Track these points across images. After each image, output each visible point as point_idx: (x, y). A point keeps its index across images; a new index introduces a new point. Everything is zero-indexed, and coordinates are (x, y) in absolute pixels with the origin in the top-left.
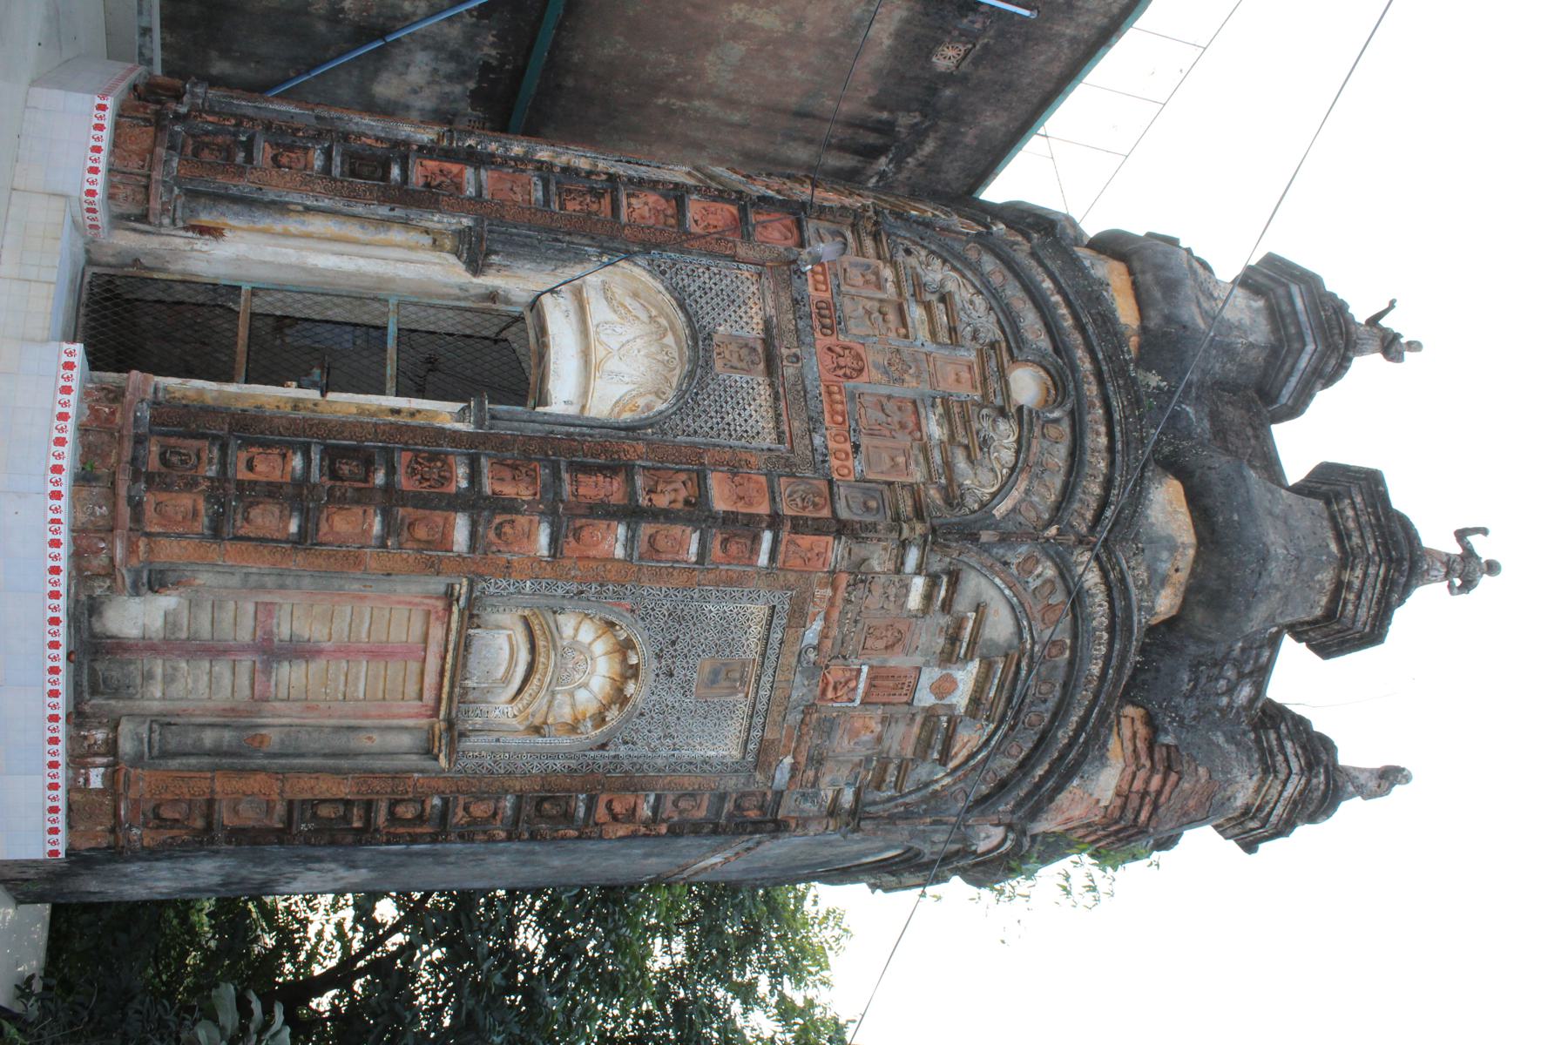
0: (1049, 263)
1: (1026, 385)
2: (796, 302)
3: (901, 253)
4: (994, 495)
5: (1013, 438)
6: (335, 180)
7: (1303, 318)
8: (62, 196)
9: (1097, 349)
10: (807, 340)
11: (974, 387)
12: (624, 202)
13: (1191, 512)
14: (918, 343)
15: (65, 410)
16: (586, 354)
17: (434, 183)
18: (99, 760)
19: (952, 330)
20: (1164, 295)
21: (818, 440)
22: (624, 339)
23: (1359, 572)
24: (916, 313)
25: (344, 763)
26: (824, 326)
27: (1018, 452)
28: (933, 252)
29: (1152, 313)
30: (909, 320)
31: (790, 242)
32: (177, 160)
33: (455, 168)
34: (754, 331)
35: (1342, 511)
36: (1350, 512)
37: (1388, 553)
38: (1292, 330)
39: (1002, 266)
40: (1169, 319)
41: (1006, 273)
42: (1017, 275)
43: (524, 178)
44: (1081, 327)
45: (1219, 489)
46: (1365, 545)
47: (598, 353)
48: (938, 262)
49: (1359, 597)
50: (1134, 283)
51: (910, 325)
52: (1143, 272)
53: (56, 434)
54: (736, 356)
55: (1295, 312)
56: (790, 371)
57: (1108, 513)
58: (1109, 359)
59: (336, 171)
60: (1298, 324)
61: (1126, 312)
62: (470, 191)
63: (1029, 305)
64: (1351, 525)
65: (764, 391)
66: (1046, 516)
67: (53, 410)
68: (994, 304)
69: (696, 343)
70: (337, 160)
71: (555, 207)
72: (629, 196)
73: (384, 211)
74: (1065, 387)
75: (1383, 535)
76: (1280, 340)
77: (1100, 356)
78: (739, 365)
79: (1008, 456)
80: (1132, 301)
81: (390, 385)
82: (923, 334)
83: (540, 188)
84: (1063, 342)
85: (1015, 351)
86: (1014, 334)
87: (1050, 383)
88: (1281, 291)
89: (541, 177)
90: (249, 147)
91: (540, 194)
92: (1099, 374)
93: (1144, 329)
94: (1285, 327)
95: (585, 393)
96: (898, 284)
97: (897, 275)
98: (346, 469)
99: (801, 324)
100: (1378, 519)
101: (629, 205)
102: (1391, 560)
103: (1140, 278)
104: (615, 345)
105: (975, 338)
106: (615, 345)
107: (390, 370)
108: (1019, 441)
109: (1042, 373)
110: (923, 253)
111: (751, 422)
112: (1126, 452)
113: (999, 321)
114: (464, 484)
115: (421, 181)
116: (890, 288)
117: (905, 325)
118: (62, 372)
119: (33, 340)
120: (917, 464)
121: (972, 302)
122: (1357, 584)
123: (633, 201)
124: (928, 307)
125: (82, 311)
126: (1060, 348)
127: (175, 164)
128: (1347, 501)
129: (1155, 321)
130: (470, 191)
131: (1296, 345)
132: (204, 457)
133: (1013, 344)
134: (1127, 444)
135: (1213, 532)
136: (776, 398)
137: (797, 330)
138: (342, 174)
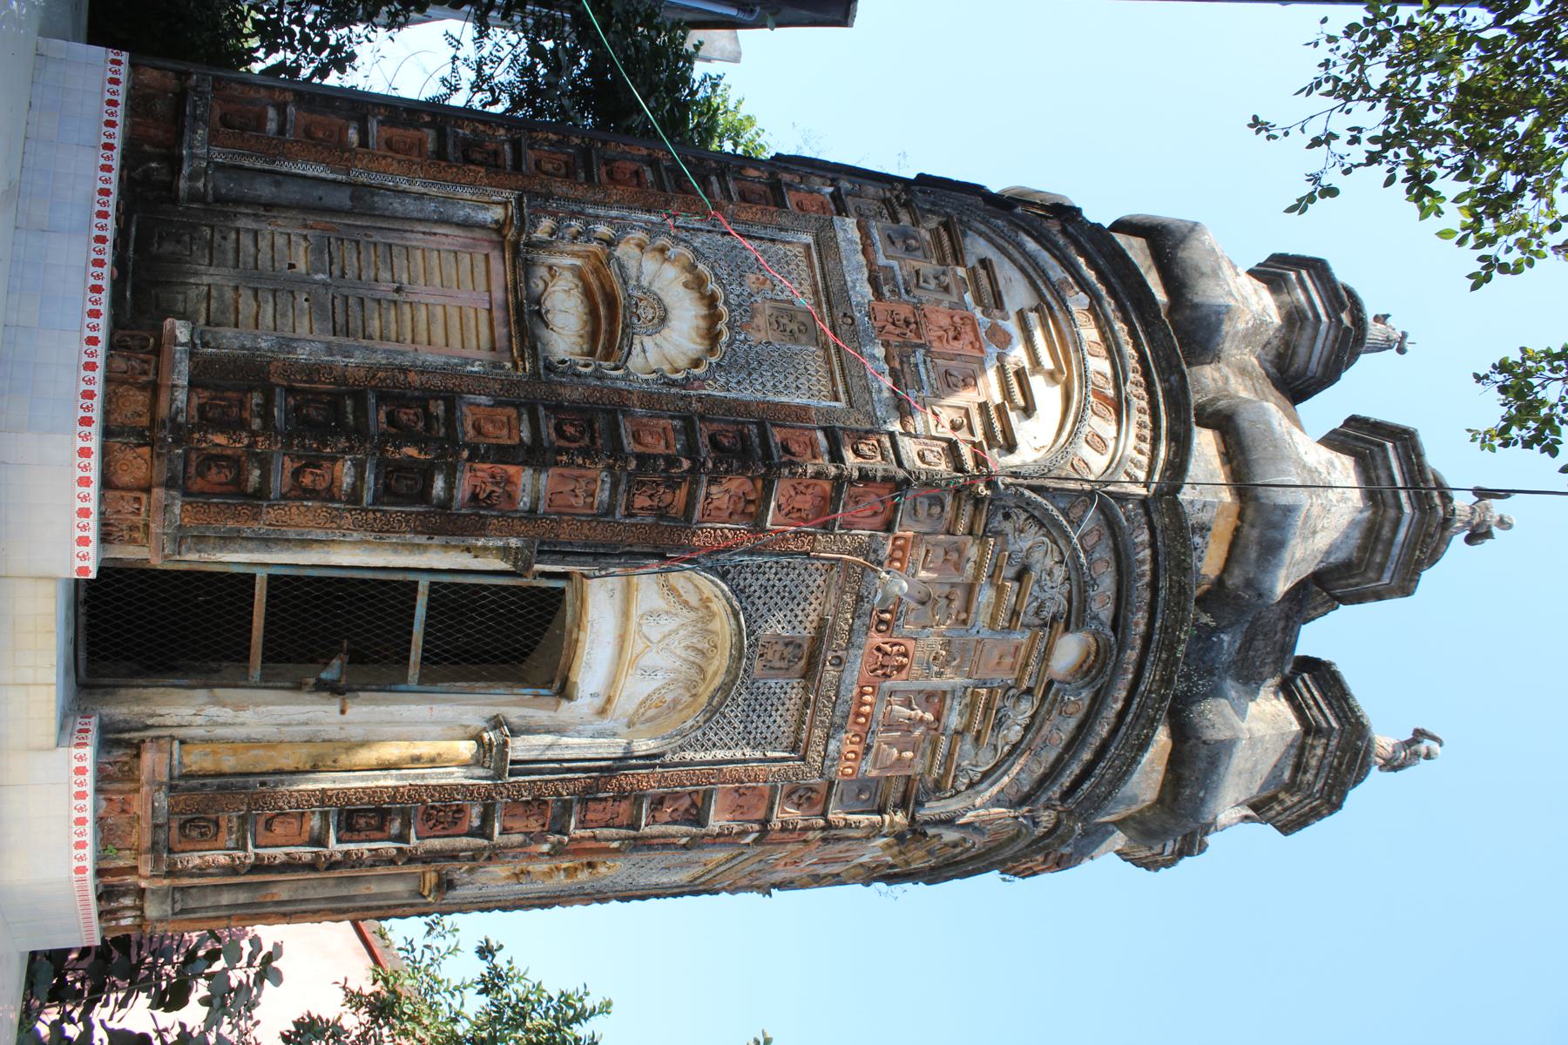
0: (1155, 517)
1: (1069, 650)
2: (860, 599)
3: (1000, 517)
4: (985, 775)
5: (1029, 713)
6: (366, 511)
7: (1396, 551)
8: (50, 578)
9: (1159, 616)
10: (857, 640)
11: (1012, 668)
12: (703, 492)
13: (1167, 771)
14: (974, 631)
15: (82, 815)
16: (622, 639)
17: (482, 496)
18: (129, 913)
19: (1015, 613)
20: (1257, 560)
21: (832, 746)
22: (666, 630)
23: (1295, 799)
24: (986, 596)
25: (344, 905)
26: (881, 621)
27: (1027, 728)
28: (1032, 516)
29: (1237, 572)
30: (975, 604)
31: (879, 520)
32: (178, 503)
33: (512, 470)
34: (806, 632)
35: (1313, 747)
36: (1319, 751)
37: (1330, 794)
38: (1378, 558)
39: (1103, 523)
40: (1249, 584)
41: (1106, 532)
42: (1114, 536)
43: (591, 474)
44: (1154, 587)
45: (1202, 765)
46: (1314, 783)
47: (635, 645)
48: (1034, 529)
49: (1285, 810)
50: (1237, 529)
51: (974, 609)
52: (1252, 526)
53: (76, 839)
54: (778, 655)
55: (1391, 542)
56: (830, 673)
57: (1085, 786)
58: (1164, 629)
59: (367, 497)
60: (1387, 555)
61: (1210, 561)
62: (524, 502)
63: (1112, 569)
64: (1314, 762)
65: (795, 694)
66: (1026, 789)
67: (70, 816)
68: (1073, 576)
69: (740, 659)
70: (370, 477)
71: (619, 513)
72: (710, 483)
73: (422, 539)
74: (1104, 664)
75: (1335, 778)
76: (1361, 560)
77: (1158, 625)
78: (777, 664)
79: (1014, 733)
80: (1225, 547)
81: (414, 671)
82: (983, 619)
83: (607, 486)
84: (1126, 618)
85: (1072, 626)
86: (1078, 610)
87: (1093, 648)
88: (1392, 513)
89: (612, 475)
90: (264, 462)
91: (605, 496)
92: (1147, 638)
93: (1220, 581)
94: (1373, 551)
95: (613, 682)
96: (979, 566)
97: (982, 555)
98: (362, 821)
99: (858, 622)
100: (1340, 764)
101: (708, 495)
102: (1329, 801)
103: (1246, 527)
104: (655, 636)
105: (1037, 614)
106: (655, 636)
107: (416, 654)
108: (1033, 717)
109: (1091, 639)
110: (1024, 516)
111: (773, 728)
112: (1132, 726)
113: (1070, 592)
114: (476, 823)
115: (467, 495)
116: (970, 568)
117: (967, 610)
118: (75, 778)
119: (40, 749)
120: (923, 756)
121: (1050, 573)
122: (1289, 803)
123: (714, 489)
124: (1000, 590)
125: (82, 610)
126: (1118, 623)
127: (177, 510)
128: (1324, 741)
129: (1235, 580)
130: (524, 502)
131: (1371, 575)
132: (223, 823)
133: (1073, 617)
134: (1137, 717)
135: (1175, 799)
136: (806, 704)
137: (851, 630)
138: (376, 500)
